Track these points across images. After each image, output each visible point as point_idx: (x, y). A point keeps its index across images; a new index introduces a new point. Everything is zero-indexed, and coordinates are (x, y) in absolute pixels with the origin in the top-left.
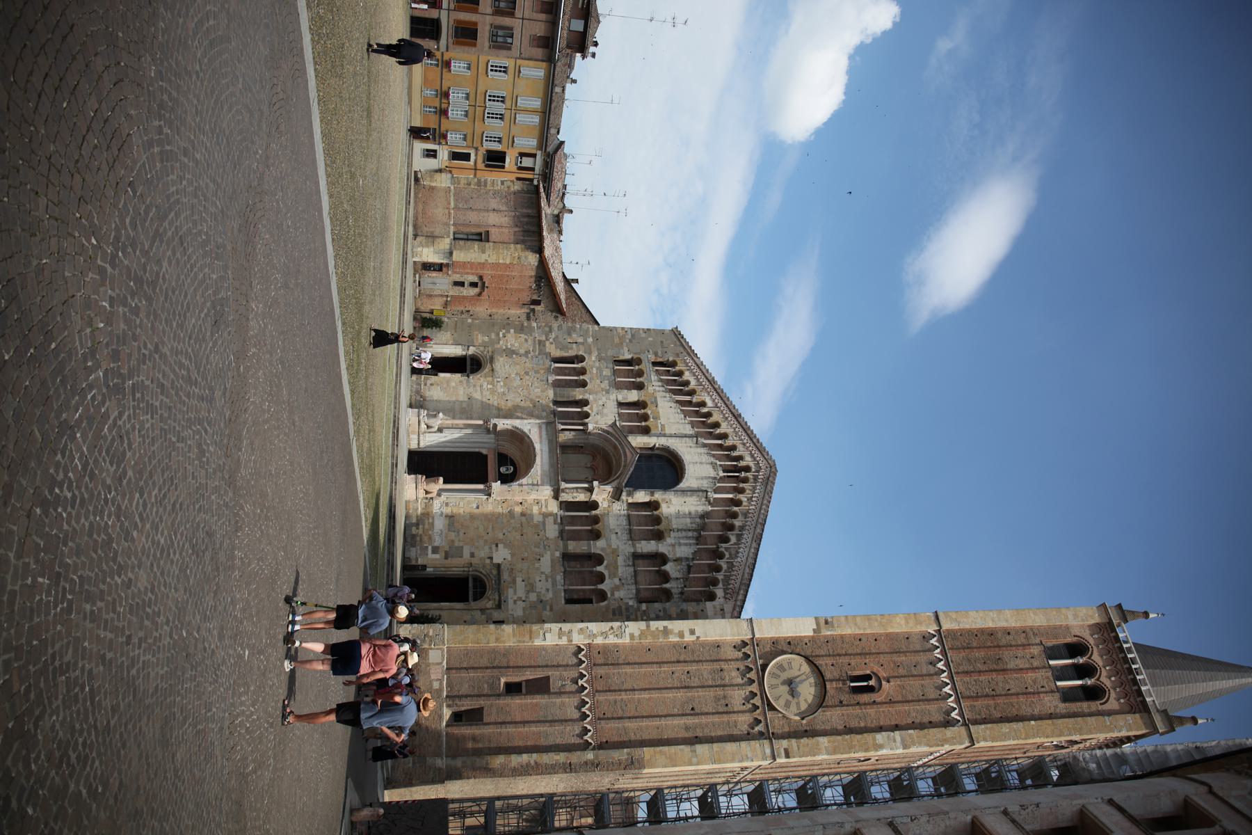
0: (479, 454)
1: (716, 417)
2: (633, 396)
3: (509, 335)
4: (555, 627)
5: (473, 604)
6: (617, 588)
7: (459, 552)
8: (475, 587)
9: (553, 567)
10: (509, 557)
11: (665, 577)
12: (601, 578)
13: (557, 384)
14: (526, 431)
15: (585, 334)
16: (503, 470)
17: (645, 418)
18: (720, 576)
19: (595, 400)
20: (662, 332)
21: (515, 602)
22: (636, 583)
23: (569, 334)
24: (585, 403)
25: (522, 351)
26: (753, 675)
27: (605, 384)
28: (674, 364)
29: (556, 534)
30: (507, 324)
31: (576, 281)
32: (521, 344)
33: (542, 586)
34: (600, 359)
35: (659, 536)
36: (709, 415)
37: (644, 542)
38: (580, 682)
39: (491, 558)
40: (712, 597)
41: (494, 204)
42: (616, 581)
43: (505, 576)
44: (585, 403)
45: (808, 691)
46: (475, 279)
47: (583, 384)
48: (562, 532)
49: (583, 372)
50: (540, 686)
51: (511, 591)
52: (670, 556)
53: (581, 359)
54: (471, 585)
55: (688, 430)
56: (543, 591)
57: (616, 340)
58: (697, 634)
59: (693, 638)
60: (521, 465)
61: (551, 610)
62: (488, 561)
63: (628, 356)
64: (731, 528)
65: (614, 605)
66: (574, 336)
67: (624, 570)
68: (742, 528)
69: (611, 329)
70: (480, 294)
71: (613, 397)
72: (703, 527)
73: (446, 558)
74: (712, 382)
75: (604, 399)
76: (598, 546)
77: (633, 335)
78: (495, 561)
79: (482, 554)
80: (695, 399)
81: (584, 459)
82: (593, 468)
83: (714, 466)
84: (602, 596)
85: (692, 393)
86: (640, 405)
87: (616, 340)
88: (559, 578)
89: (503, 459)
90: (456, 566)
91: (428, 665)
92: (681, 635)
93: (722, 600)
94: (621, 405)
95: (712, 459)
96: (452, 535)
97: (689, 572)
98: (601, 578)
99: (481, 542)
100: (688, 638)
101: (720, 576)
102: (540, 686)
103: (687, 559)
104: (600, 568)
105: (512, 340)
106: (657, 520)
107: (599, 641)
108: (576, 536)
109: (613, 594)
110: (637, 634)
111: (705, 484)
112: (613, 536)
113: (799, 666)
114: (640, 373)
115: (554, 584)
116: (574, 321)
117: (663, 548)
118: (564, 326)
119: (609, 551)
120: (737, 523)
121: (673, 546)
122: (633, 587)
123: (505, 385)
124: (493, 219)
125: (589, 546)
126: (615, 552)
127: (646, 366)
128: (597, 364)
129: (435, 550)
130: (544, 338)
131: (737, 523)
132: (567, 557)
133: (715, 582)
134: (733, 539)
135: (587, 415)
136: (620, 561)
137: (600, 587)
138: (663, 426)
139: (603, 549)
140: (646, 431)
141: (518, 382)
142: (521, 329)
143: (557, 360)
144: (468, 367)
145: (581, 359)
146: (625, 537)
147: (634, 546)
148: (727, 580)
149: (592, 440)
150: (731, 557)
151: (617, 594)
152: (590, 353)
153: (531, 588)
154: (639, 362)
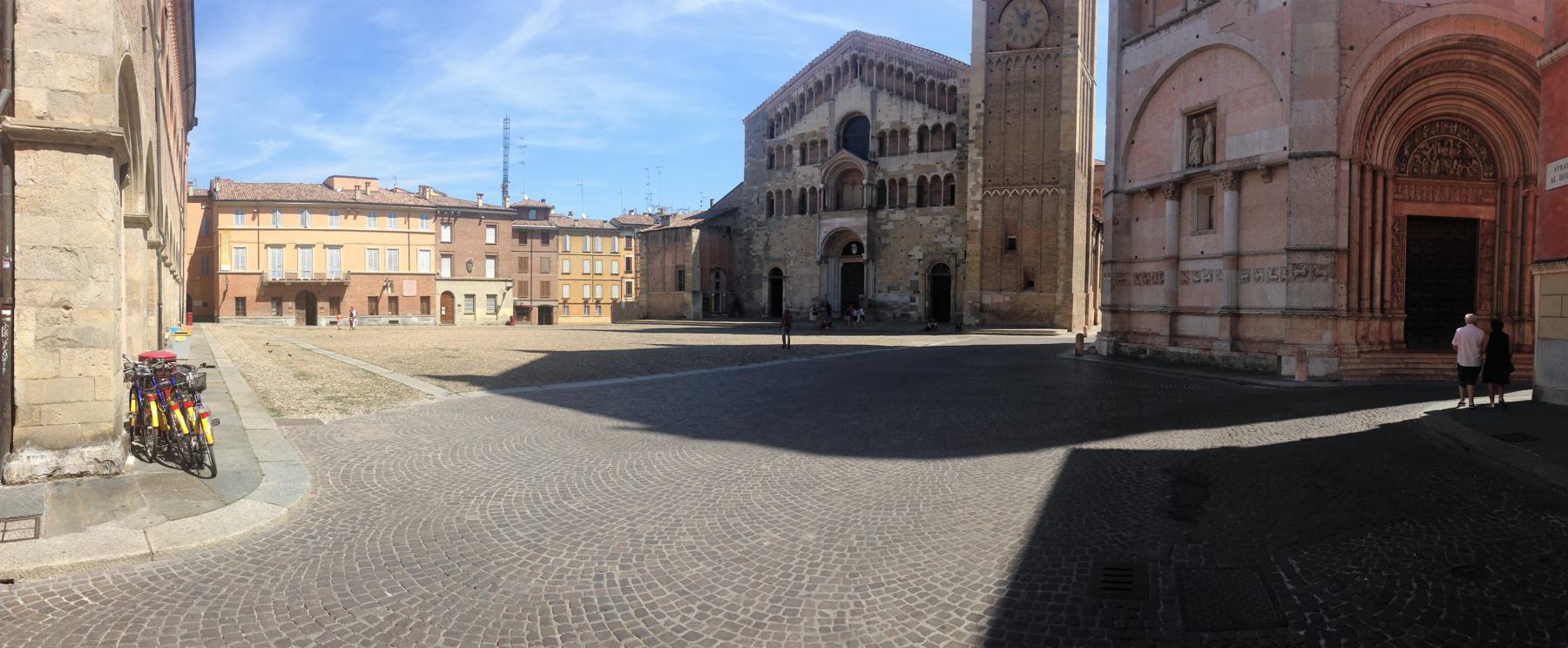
1: (811, 85)
2: (797, 153)
4: (969, 214)
5: (952, 272)
11: (937, 127)
12: (936, 178)
17: (814, 143)
18: (938, 81)
20: (747, 132)
24: (803, 190)
28: (772, 121)
30: (747, 250)
33: (940, 223)
34: (769, 180)
35: (905, 132)
36: (810, 91)
40: (953, 89)
41: (657, 263)
43: (932, 249)
44: (803, 190)
46: (713, 275)
47: (789, 192)
48: (901, 208)
49: (779, 193)
55: (825, 107)
60: (850, 239)
63: (766, 159)
64: (900, 71)
65: (956, 168)
67: (930, 159)
68: (901, 61)
72: (899, 93)
74: (785, 88)
76: (912, 180)
79: (915, 267)
80: (798, 104)
81: (847, 191)
82: (854, 184)
84: (949, 177)
85: (793, 106)
88: (935, 209)
89: (847, 251)
90: (923, 284)
92: (979, 115)
94: (803, 163)
98: (936, 178)
100: (981, 110)
101: (938, 81)
105: (757, 247)
106: (894, 132)
108: (904, 198)
111: (867, 93)
114: (780, 148)
117: (914, 129)
120: (897, 66)
124: (669, 263)
126: (917, 167)
129: (913, 300)
132: (920, 203)
133: (942, 87)
134: (910, 69)
135: (813, 189)
136: (923, 163)
140: (825, 142)
142: (749, 240)
143: (770, 213)
146: (905, 158)
148: (940, 76)
149: (832, 183)
153: (942, 230)
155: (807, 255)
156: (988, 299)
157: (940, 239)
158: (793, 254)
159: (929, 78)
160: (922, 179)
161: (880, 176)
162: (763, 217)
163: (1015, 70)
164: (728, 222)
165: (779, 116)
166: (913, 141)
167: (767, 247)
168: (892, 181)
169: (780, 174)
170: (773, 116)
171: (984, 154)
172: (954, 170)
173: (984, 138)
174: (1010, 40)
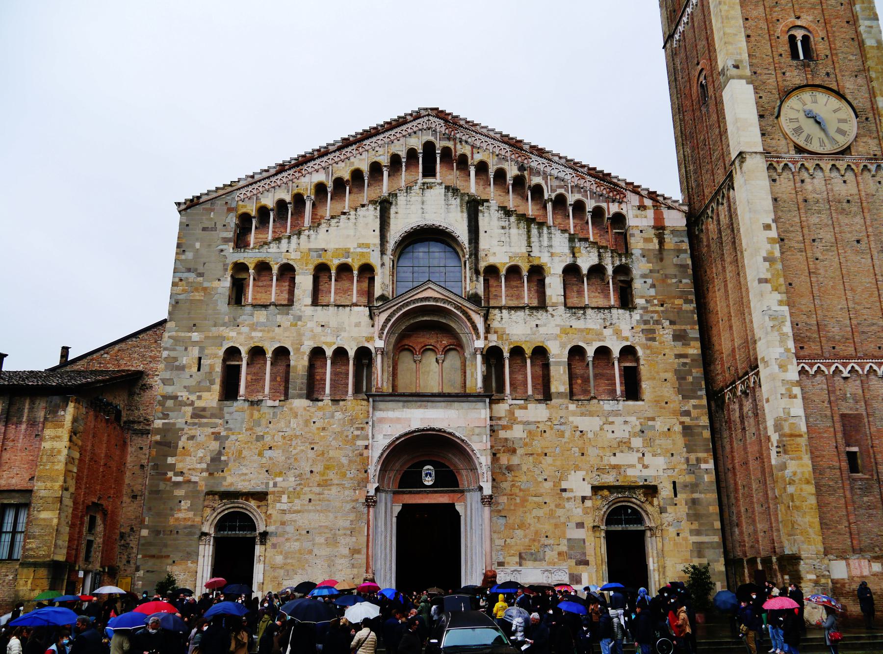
0: (399, 517)
2: (304, 282)
3: (179, 466)
6: (617, 333)
7: (576, 545)
8: (619, 522)
9: (591, 414)
10: (581, 474)
11: (597, 271)
12: (603, 352)
13: (284, 390)
14: (387, 442)
15: (186, 344)
16: (428, 481)
17: (344, 269)
18: (590, 204)
19: (314, 337)
20: (184, 227)
21: (646, 467)
22: (610, 308)
23: (182, 368)
24: (317, 353)
25: (215, 445)
26: (810, 165)
27: (285, 320)
28: (245, 219)
29: (542, 406)
30: (160, 469)
31: (65, 350)
32: (199, 446)
33: (621, 431)
35: (537, 273)
37: (548, 292)
38: (845, 374)
39: (584, 499)
40: (619, 219)
42: (608, 332)
43: (610, 479)
45: (825, 105)
47: (282, 353)
48: (539, 401)
49: (257, 352)
50: (851, 426)
51: (630, 472)
52: (569, 260)
53: (233, 353)
54: (619, 528)
56: (628, 428)
57: (198, 296)
58: (770, 222)
59: (774, 226)
61: (653, 419)
62: (588, 503)
63: (227, 283)
64: (519, 182)
66: (185, 361)
67: (593, 321)
68: (522, 168)
69: (175, 304)
70: (105, 514)
71: (310, 311)
73: (587, 563)
75: (310, 325)
76: (558, 353)
77: (189, 270)
78: (588, 492)
79: (577, 512)
82: (425, 350)
83: (426, 187)
84: (628, 352)
85: (299, 199)
86: (321, 270)
87: (198, 296)
88: (608, 406)
90: (597, 548)
91: (851, 578)
92: (771, 241)
93: (623, 206)
94: (315, 302)
95: (416, 188)
96: (551, 555)
97: (586, 240)
98: (603, 352)
99: (560, 512)
100: (773, 234)
101: (590, 204)
102: (851, 426)
103: (571, 239)
104: (590, 352)
105: (191, 462)
106: (514, 271)
107: (791, 344)
109: (627, 339)
110: (777, 296)
112: (542, 330)
113: (793, 108)
114: (263, 267)
115: (617, 413)
116: (154, 359)
118: (167, 375)
119: (564, 338)
121: (552, 255)
122: (614, 311)
123: (280, 474)
125: (558, 363)
126: (566, 331)
127: (250, 257)
128: (245, 329)
130: (189, 410)
131: (512, 171)
132: (571, 395)
133: (598, 213)
134: (536, 180)
137: (616, 353)
138: (360, 245)
139: (563, 346)
140: (367, 270)
141: (277, 455)
142: (168, 444)
143: (229, 391)
144: (249, 534)
145: (233, 353)
146: (541, 314)
147: (554, 305)
150: (565, 187)
151: (626, 333)
152: (224, 338)
153: (624, 445)
154: (240, 267)
155: (325, 484)
156: (839, 570)
157: (621, 459)
158: (291, 481)
159: (571, 199)
160: (577, 352)
161: (493, 340)
162: (211, 398)
163: (815, 185)
164: (119, 401)
165: (263, 212)
166: (554, 286)
167: (216, 464)
168: (517, 352)
169: (261, 316)
170: (251, 209)
171: (790, 304)
172: (638, 342)
173: (785, 277)
174: (801, 142)
